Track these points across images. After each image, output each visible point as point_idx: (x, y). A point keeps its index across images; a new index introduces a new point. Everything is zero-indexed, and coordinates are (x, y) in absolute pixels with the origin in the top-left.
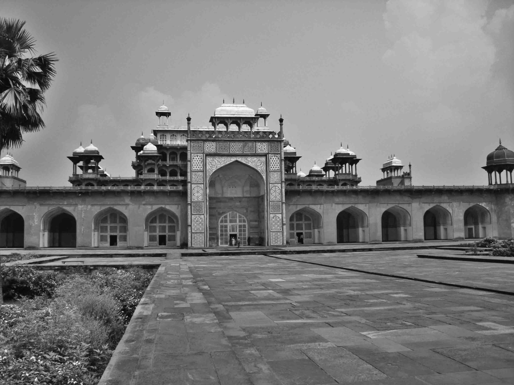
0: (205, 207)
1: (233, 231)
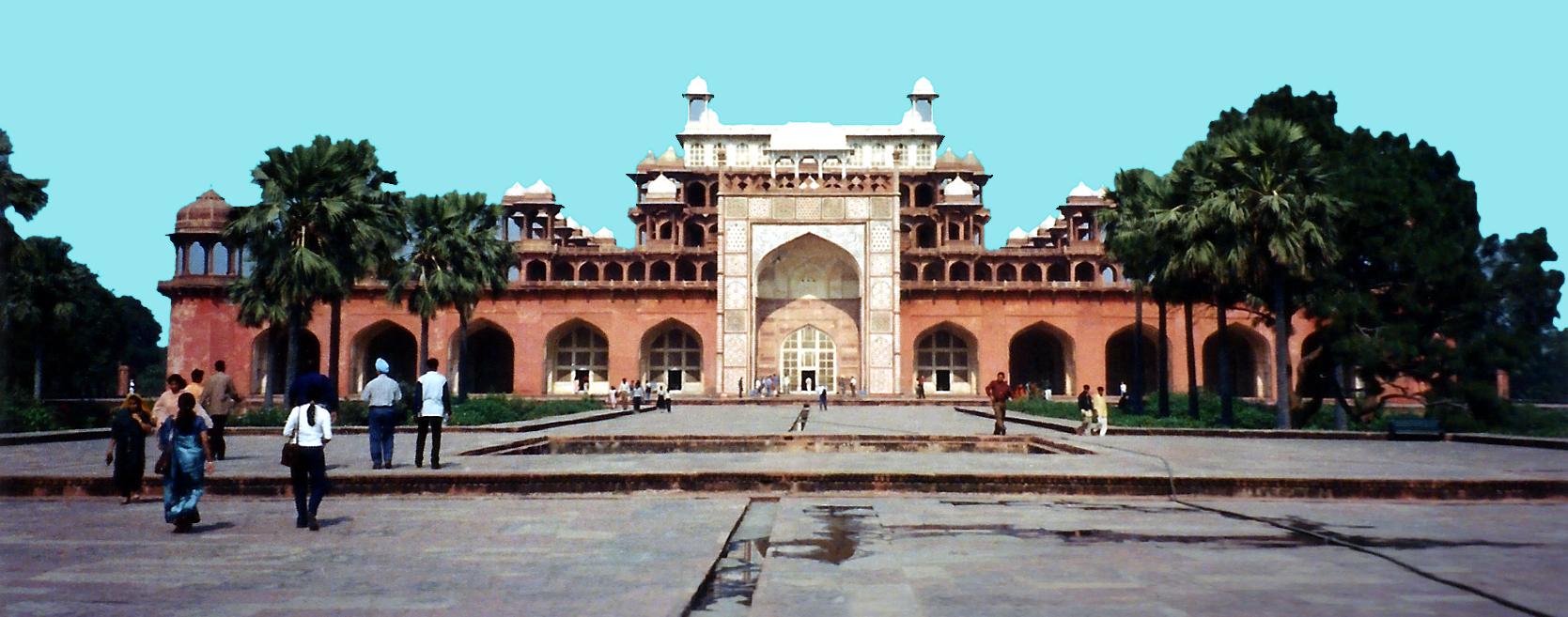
0: (749, 317)
1: (808, 364)
